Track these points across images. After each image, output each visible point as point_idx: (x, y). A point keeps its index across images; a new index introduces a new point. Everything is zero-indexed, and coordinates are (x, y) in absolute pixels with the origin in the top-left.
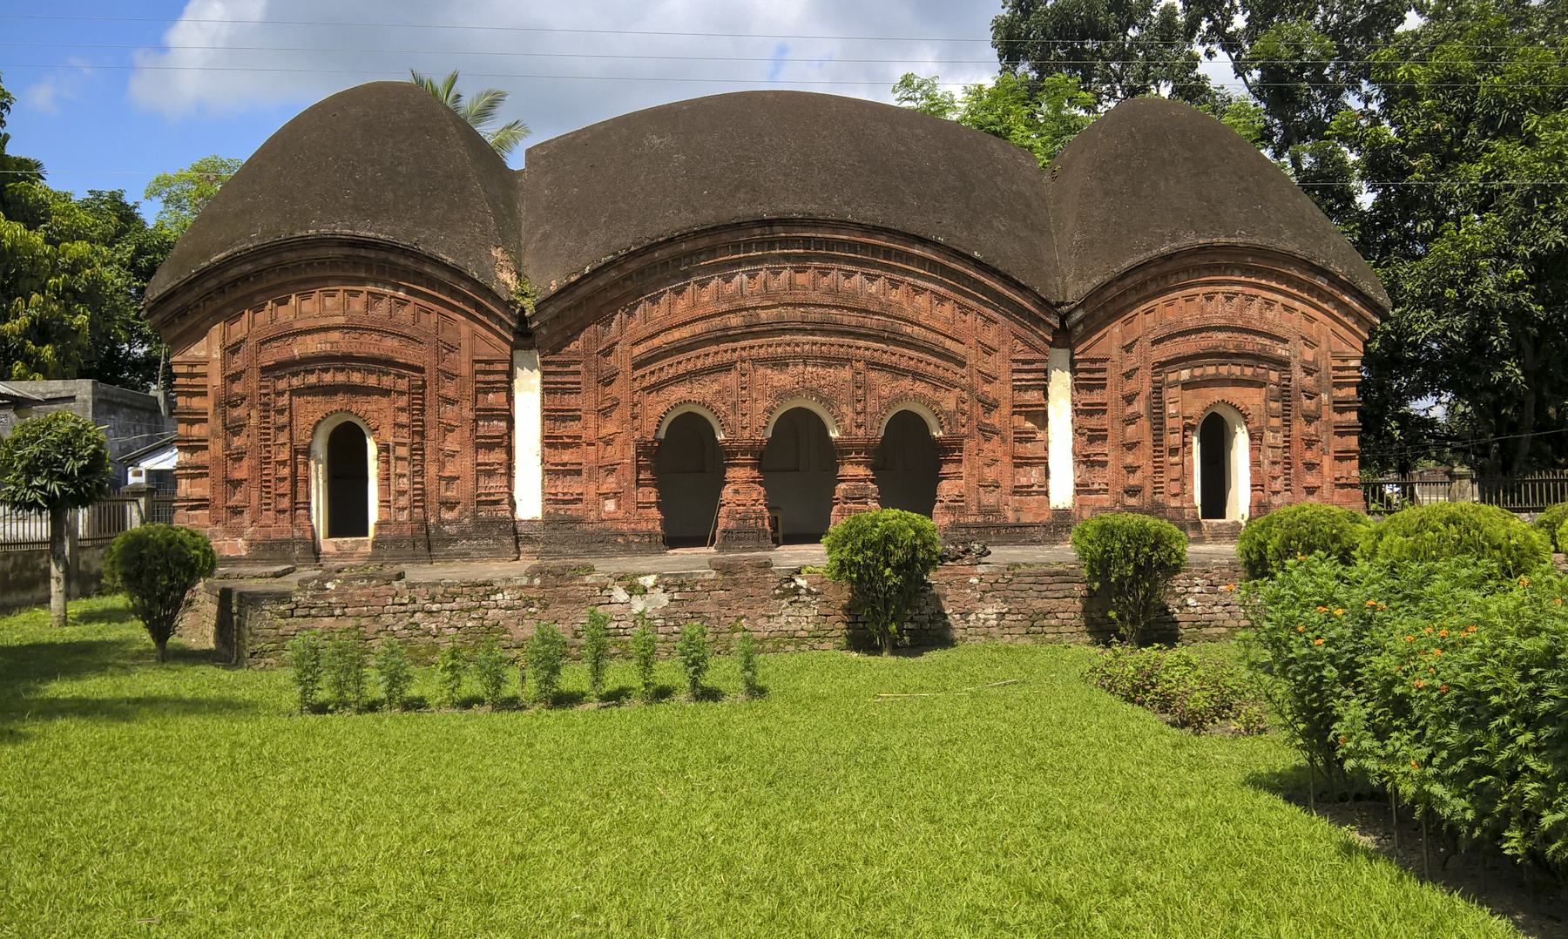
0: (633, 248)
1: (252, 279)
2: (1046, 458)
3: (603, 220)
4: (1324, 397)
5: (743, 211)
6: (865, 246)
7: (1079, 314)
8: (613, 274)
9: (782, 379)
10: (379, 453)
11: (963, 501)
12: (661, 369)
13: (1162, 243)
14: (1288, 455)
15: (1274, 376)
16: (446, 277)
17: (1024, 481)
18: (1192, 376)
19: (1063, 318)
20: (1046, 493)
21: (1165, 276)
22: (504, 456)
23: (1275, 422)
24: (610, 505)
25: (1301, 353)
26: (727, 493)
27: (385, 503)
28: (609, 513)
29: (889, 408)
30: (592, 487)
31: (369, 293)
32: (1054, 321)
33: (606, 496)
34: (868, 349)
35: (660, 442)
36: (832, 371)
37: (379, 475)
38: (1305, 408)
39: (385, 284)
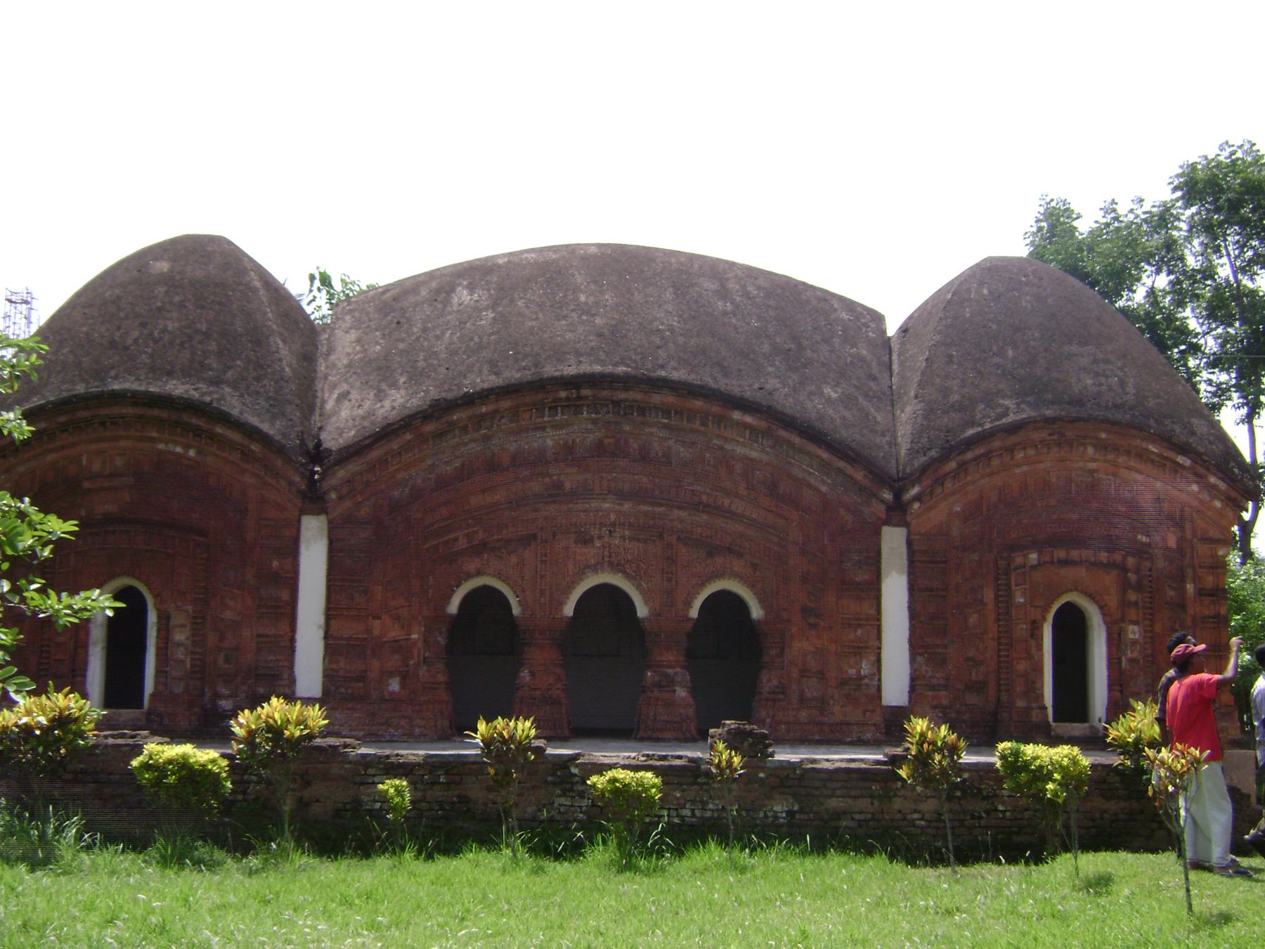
0: (430, 410)
1: (45, 437)
2: (880, 648)
3: (402, 380)
4: (1190, 587)
5: (550, 370)
6: (679, 412)
7: (915, 491)
8: (408, 436)
9: (590, 553)
10: (159, 617)
11: (783, 693)
12: (456, 539)
13: (1005, 414)
14: (1149, 652)
15: (1131, 561)
16: (236, 437)
17: (852, 672)
18: (1040, 564)
19: (898, 495)
20: (879, 689)
21: (1011, 450)
22: (287, 629)
23: (1132, 613)
24: (395, 685)
25: (1164, 540)
26: (525, 674)
27: (159, 672)
28: (393, 693)
29: (702, 585)
30: (376, 664)
31: (161, 452)
32: (888, 496)
33: (391, 674)
34: (681, 521)
35: (450, 616)
36: (640, 545)
37: (157, 643)
38: (1169, 599)
39: (176, 443)
